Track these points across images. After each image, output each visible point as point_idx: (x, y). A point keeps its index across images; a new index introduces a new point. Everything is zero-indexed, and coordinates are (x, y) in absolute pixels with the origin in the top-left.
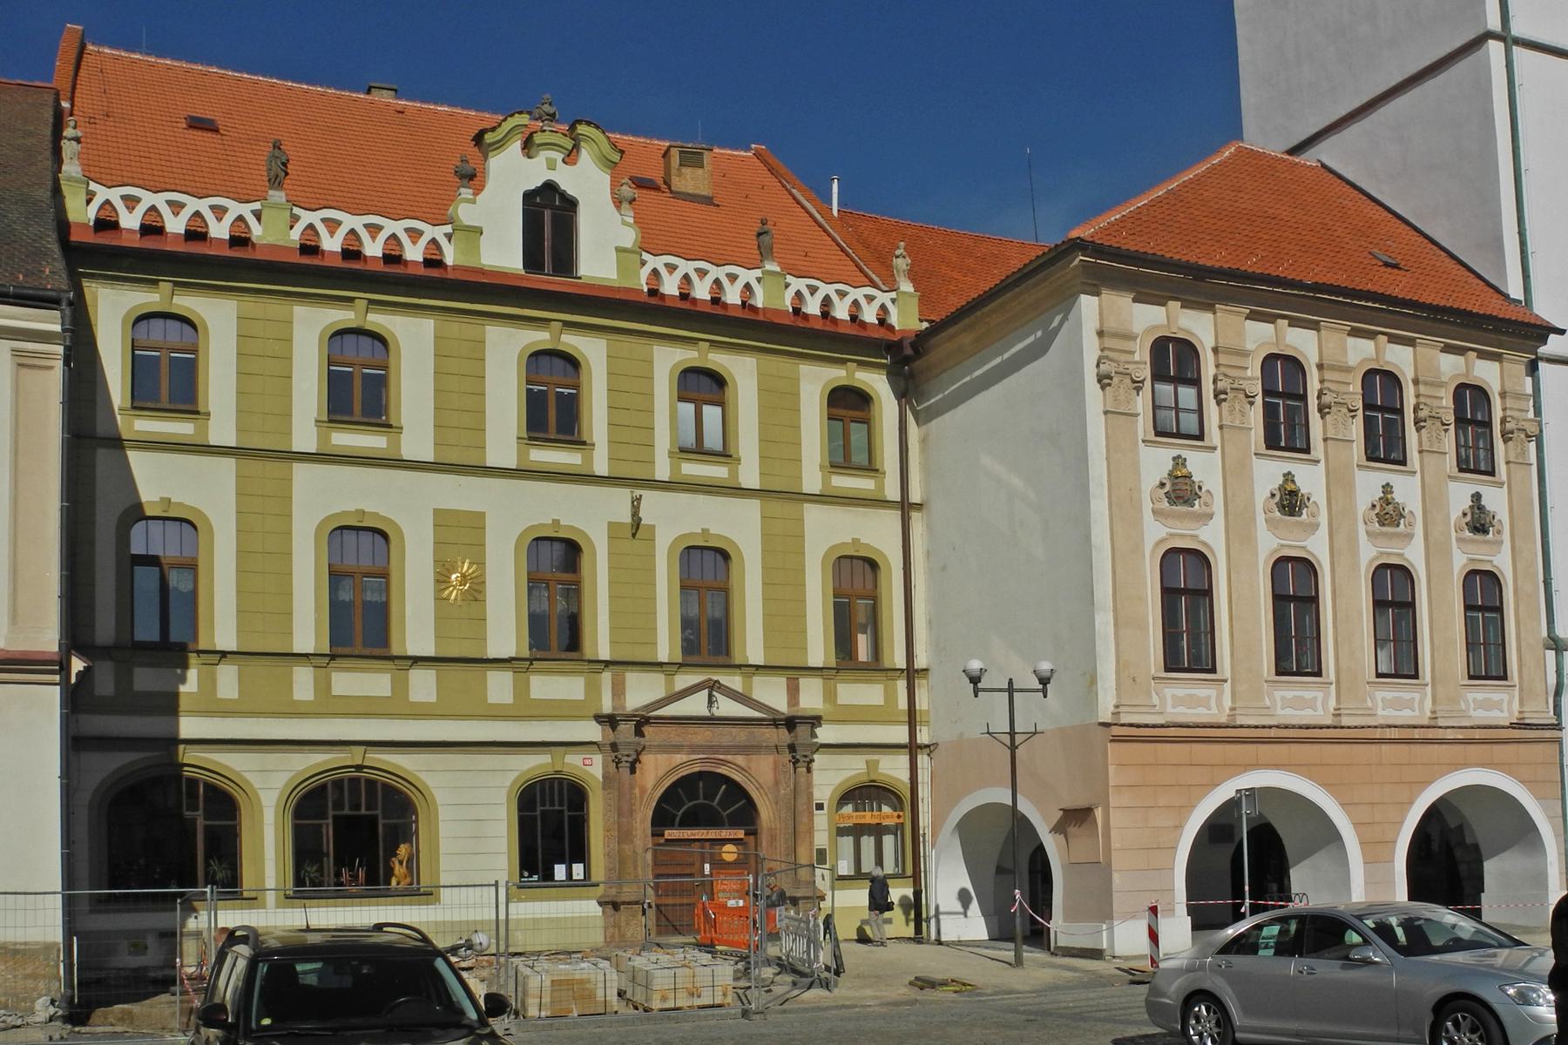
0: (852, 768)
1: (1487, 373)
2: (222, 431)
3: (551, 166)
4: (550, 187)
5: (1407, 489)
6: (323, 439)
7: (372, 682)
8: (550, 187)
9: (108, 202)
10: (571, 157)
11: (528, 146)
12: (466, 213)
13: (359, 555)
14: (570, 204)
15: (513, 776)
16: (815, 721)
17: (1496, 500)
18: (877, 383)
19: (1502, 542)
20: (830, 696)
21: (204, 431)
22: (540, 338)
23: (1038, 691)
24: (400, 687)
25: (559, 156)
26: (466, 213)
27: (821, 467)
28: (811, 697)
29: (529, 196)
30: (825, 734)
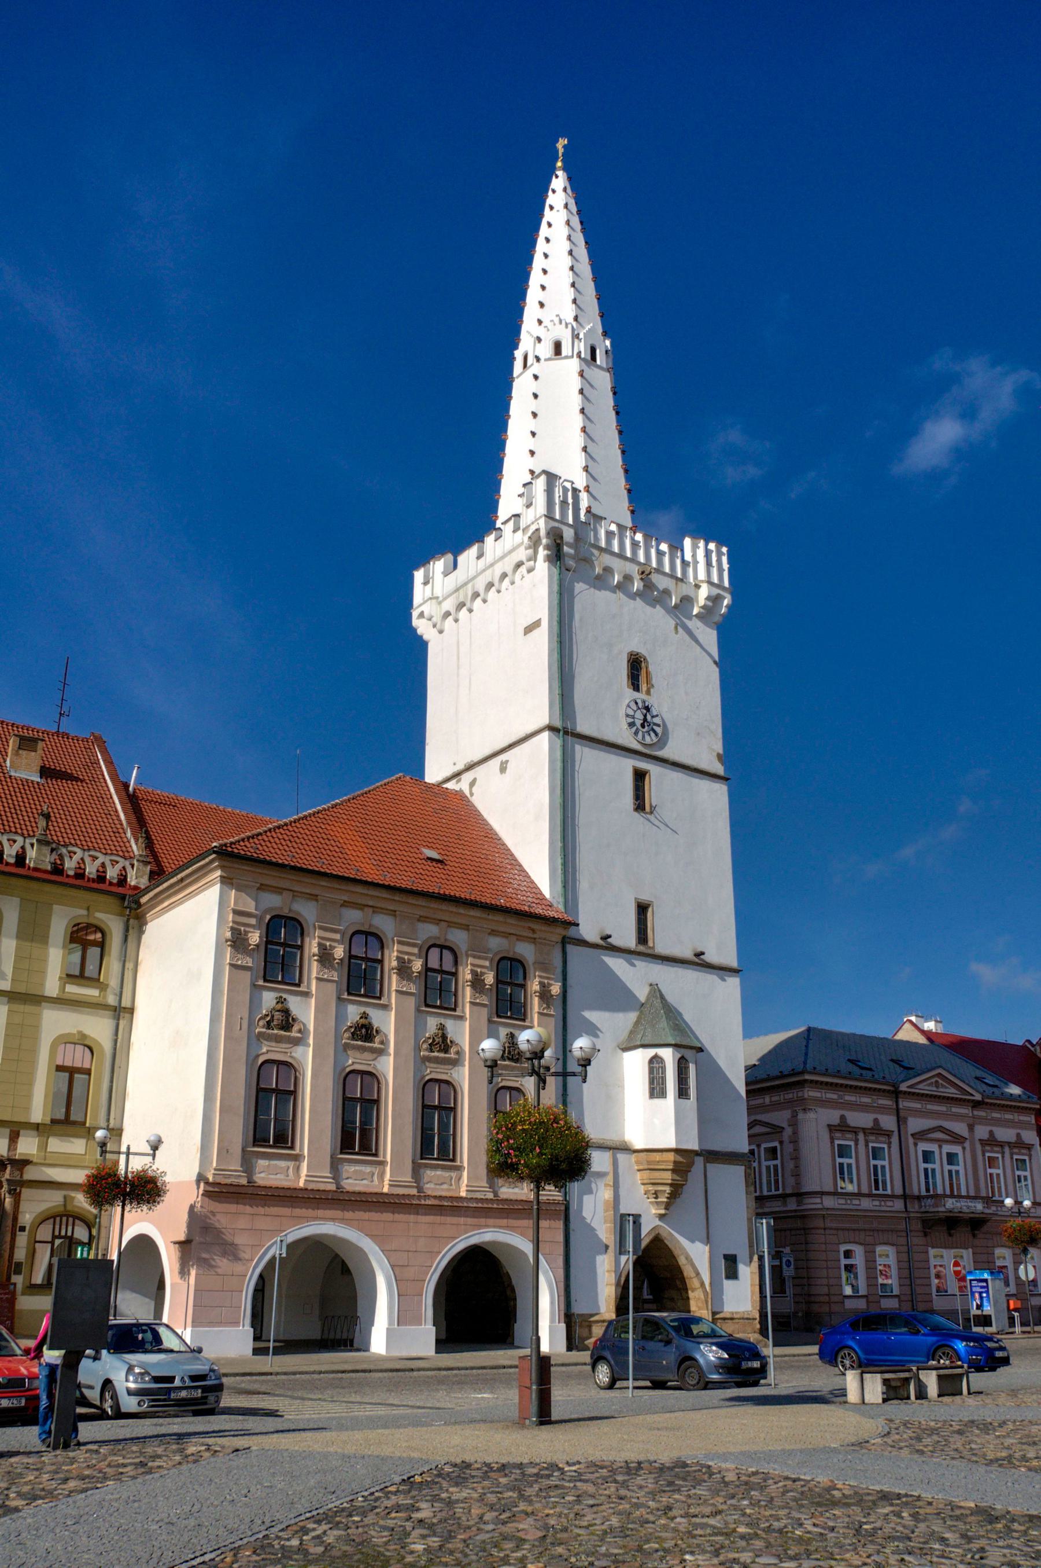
0: (53, 1200)
16: (24, 1163)
18: (114, 925)
20: (43, 1147)
23: (148, 1155)
27: (60, 978)
28: (27, 1146)
30: (30, 1173)
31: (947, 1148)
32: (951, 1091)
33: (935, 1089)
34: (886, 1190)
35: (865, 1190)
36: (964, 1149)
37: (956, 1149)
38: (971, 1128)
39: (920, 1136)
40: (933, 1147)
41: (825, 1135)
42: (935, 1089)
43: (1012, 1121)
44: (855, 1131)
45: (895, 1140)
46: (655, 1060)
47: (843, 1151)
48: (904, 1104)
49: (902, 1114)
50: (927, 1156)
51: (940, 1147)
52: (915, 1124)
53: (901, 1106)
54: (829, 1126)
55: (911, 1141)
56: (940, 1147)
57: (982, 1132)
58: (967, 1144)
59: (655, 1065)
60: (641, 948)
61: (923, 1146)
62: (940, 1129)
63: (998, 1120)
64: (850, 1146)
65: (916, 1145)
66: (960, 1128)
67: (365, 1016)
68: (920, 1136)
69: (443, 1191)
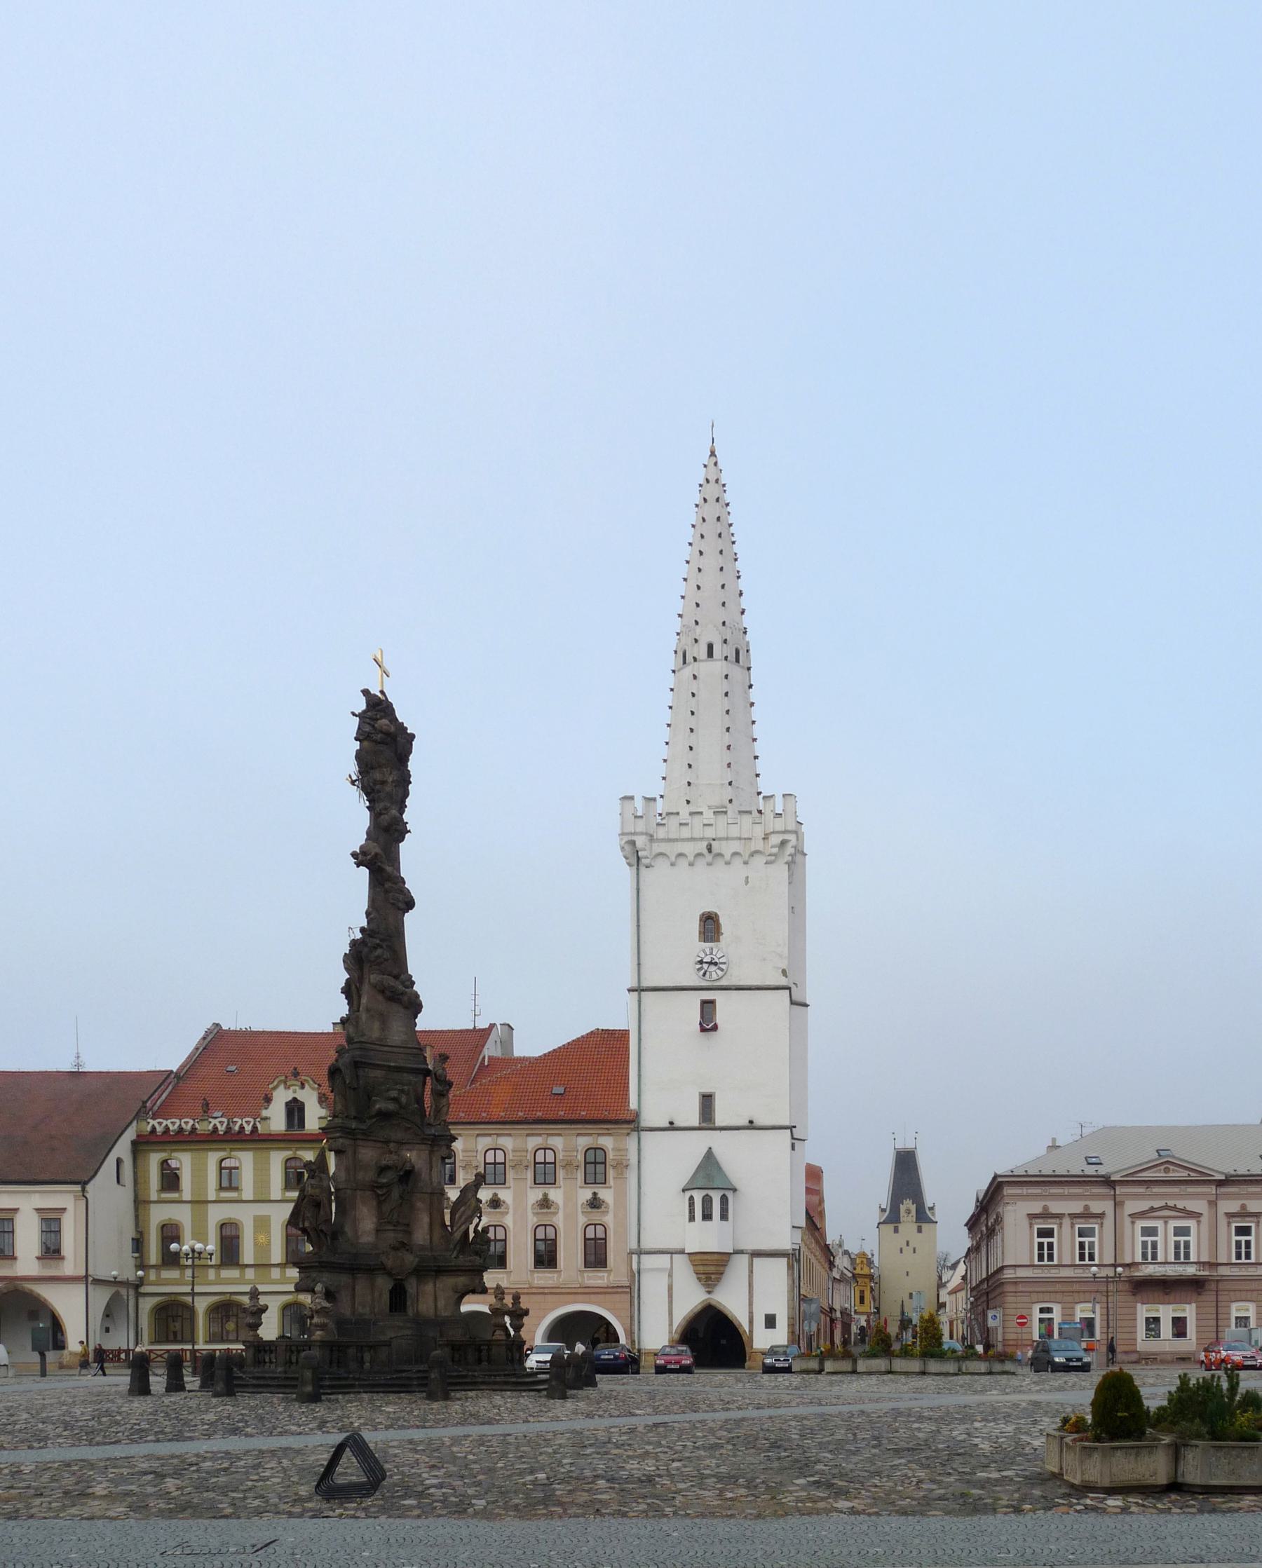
1: (607, 1142)
2: (187, 1195)
3: (295, 1092)
4: (295, 1100)
5: (555, 1195)
6: (218, 1195)
7: (233, 1273)
8: (295, 1100)
9: (153, 1125)
10: (302, 1086)
11: (287, 1088)
12: (264, 1113)
13: (227, 1232)
14: (302, 1105)
15: (279, 1303)
17: (606, 1194)
19: (608, 1212)
21: (181, 1196)
22: (289, 1154)
24: (243, 1275)
25: (297, 1088)
26: (264, 1113)
29: (287, 1104)
31: (1173, 1224)
32: (1182, 1174)
33: (1164, 1175)
34: (1094, 1260)
35: (1066, 1261)
36: (1199, 1222)
37: (1191, 1223)
38: (1213, 1204)
39: (1135, 1216)
40: (1159, 1224)
41: (1026, 1222)
42: (1164, 1175)
43: (1233, 1194)
44: (1059, 1216)
45: (1109, 1222)
46: (691, 1198)
47: (1048, 1233)
48: (1119, 1190)
49: (1117, 1200)
50: (1150, 1232)
51: (1166, 1223)
52: (1132, 1207)
53: (1117, 1193)
54: (1028, 1214)
55: (1128, 1221)
56: (1166, 1223)
57: (1234, 1206)
58: (1204, 1220)
59: (707, 1201)
60: (704, 1125)
61: (1141, 1224)
62: (1166, 1207)
63: (1253, 1193)
64: (1053, 1229)
65: (1133, 1223)
66: (1198, 1206)
67: (495, 1195)
68: (1135, 1216)
69: (550, 1283)
